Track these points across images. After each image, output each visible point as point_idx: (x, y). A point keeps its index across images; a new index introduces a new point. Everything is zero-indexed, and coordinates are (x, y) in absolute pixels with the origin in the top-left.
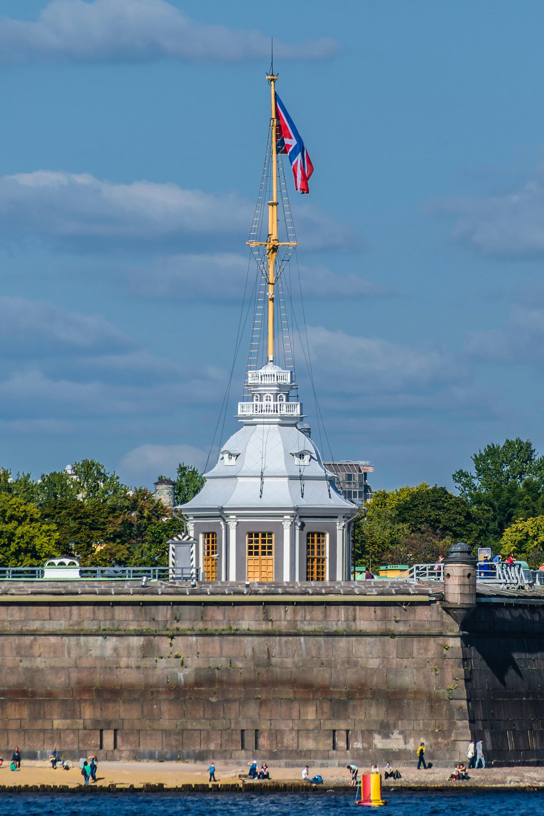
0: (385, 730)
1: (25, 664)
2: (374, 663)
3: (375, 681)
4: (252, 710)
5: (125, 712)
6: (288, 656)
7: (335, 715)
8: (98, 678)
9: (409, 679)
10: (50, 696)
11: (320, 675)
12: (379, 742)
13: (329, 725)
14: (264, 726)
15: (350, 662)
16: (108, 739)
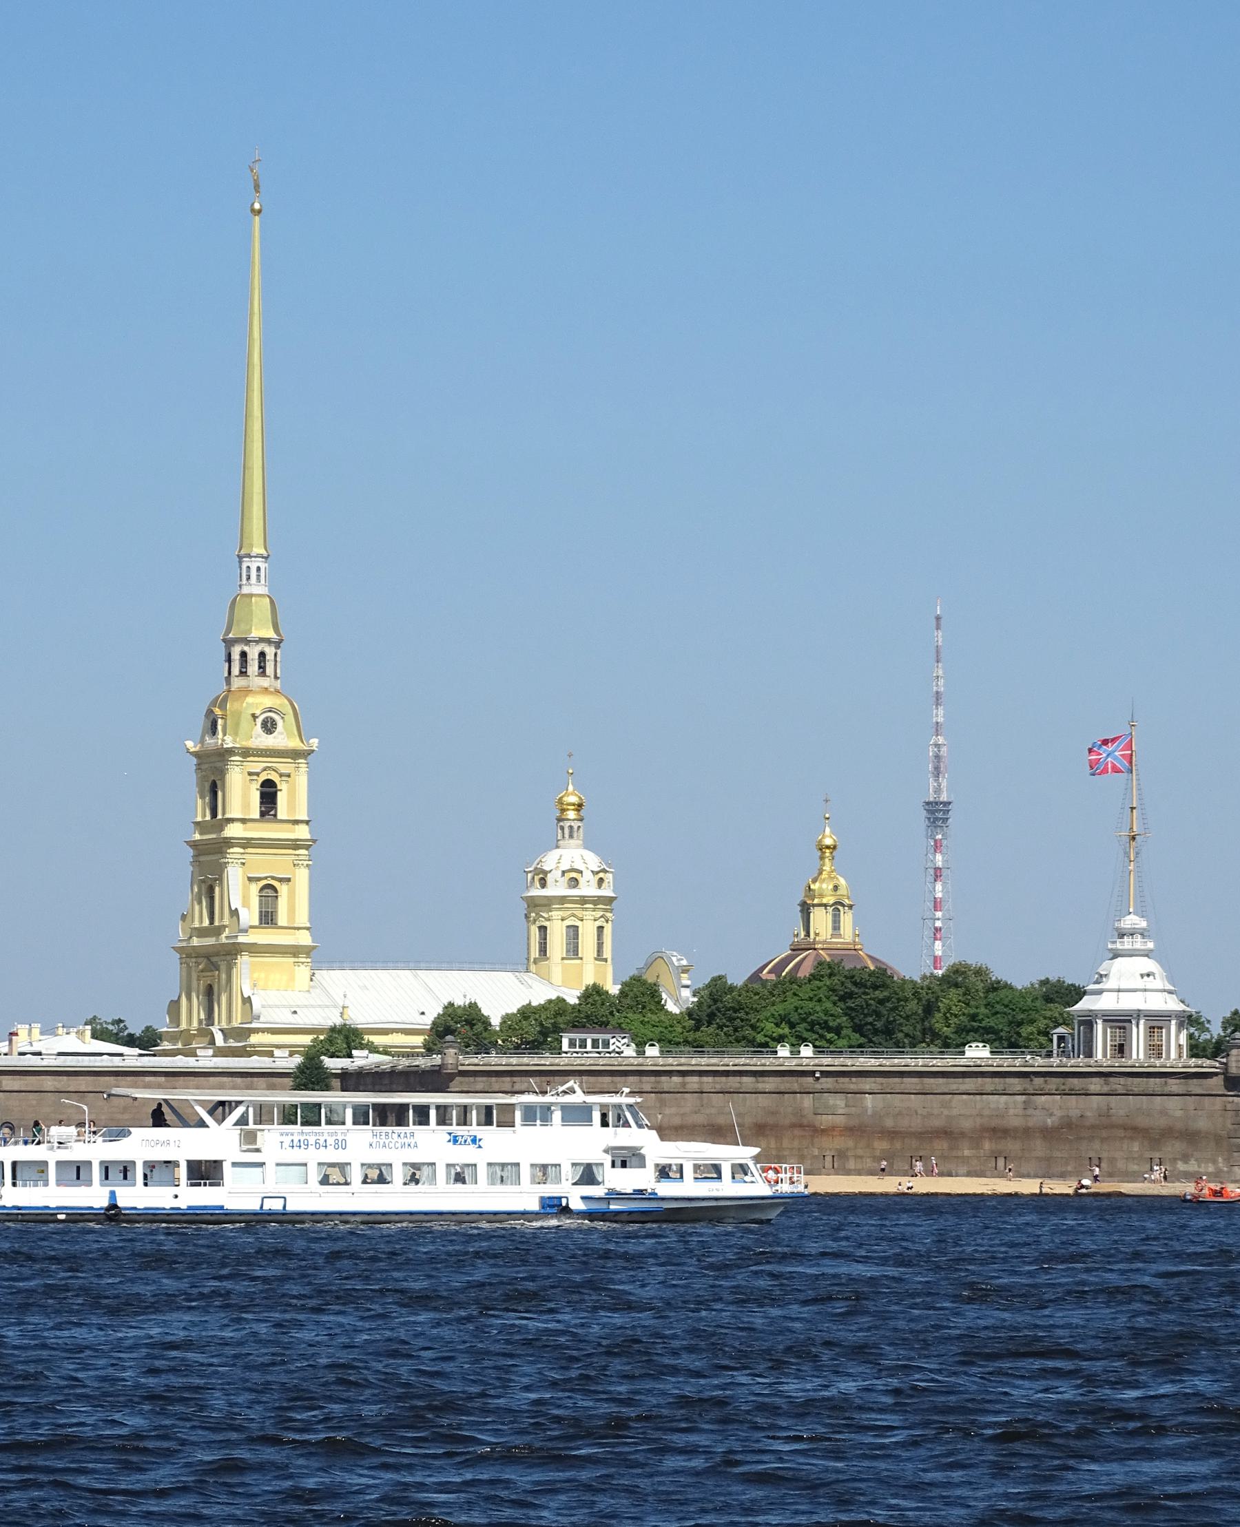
0: (1185, 1158)
1: (946, 1112)
2: (1179, 1113)
3: (1179, 1125)
4: (1097, 1145)
5: (1012, 1146)
6: (1121, 1107)
7: (1152, 1149)
8: (995, 1123)
9: (1202, 1124)
10: (963, 1134)
11: (1142, 1122)
12: (1181, 1166)
13: (1148, 1155)
14: (1104, 1155)
15: (1164, 1112)
16: (1001, 1162)
